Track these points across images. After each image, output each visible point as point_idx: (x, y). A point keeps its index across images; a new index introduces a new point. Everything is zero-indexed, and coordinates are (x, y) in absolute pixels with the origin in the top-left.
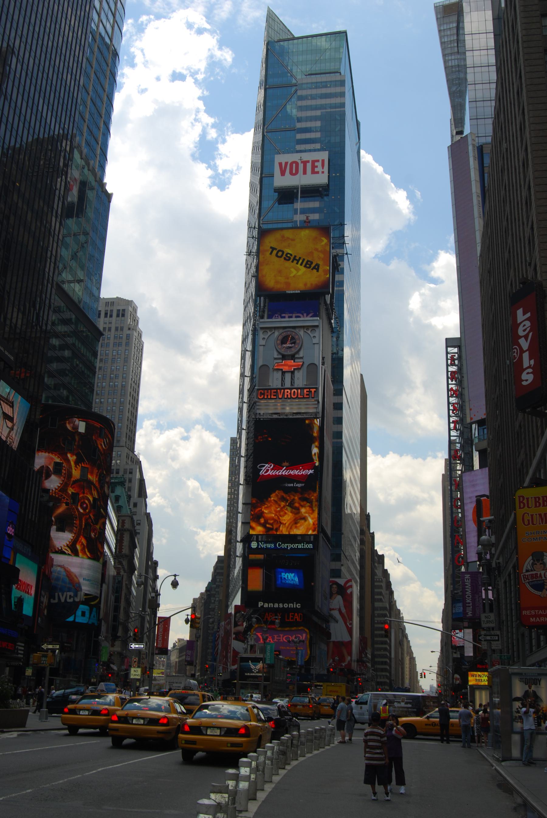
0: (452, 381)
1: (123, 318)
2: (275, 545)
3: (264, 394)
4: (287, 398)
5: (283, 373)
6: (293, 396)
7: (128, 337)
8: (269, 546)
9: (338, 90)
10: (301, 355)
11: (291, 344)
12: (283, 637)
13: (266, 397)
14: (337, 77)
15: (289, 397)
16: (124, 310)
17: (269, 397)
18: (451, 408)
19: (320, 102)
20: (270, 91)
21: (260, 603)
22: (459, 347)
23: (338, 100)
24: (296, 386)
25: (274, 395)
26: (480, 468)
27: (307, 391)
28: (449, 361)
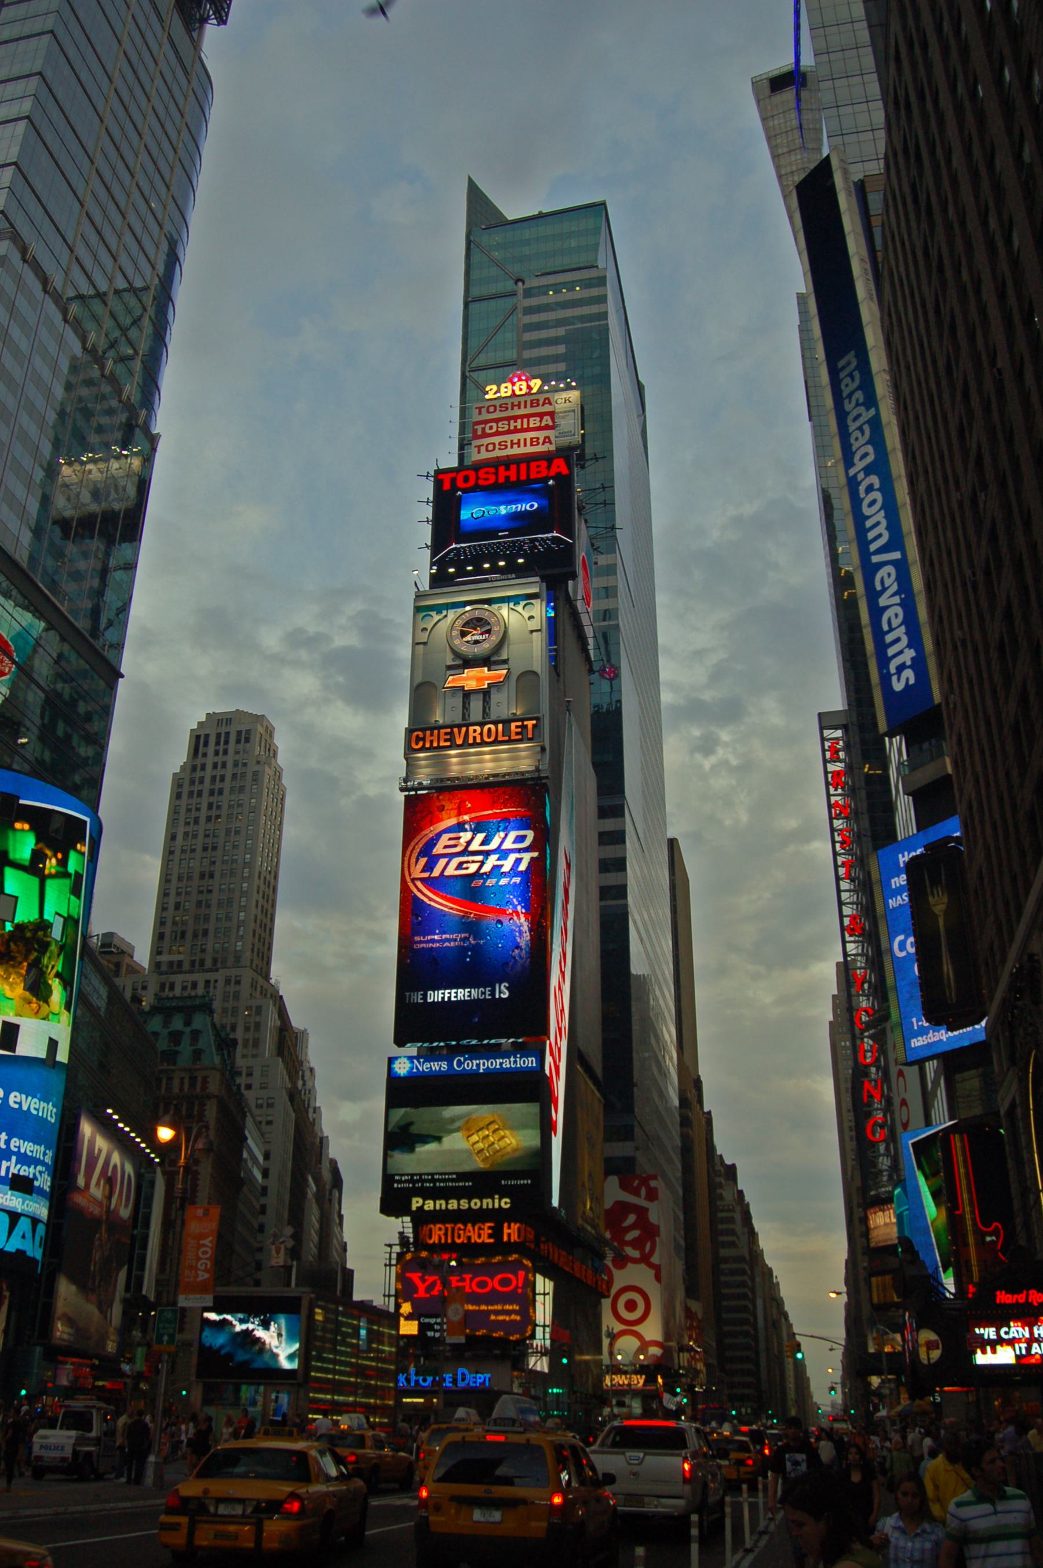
0: (836, 790)
1: (248, 745)
2: (450, 1065)
3: (424, 739)
4: (475, 744)
5: (467, 695)
6: (486, 739)
7: (256, 777)
8: (435, 1066)
9: (595, 292)
10: (505, 657)
11: (482, 634)
12: (471, 1280)
13: (428, 745)
14: (592, 273)
15: (478, 740)
16: (248, 732)
17: (435, 744)
18: (838, 838)
19: (561, 314)
20: (474, 307)
21: (414, 1200)
22: (845, 728)
23: (595, 309)
24: (493, 717)
25: (446, 740)
26: (919, 828)
27: (517, 727)
28: (828, 754)
